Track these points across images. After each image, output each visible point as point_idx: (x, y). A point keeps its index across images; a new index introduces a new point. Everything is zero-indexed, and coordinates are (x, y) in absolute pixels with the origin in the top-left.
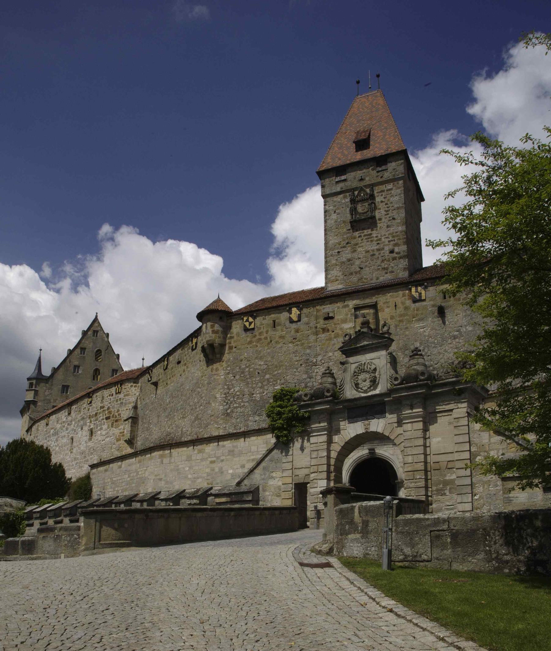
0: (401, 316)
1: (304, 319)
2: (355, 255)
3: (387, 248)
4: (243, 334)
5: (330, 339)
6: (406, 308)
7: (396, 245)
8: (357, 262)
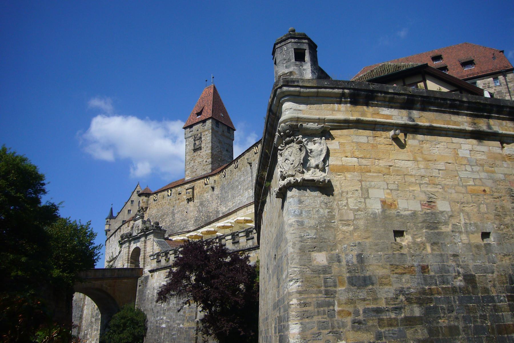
0: (202, 191)
1: (172, 195)
2: (195, 164)
3: (205, 160)
4: (154, 202)
5: (180, 203)
6: (203, 188)
7: (208, 159)
8: (195, 167)
